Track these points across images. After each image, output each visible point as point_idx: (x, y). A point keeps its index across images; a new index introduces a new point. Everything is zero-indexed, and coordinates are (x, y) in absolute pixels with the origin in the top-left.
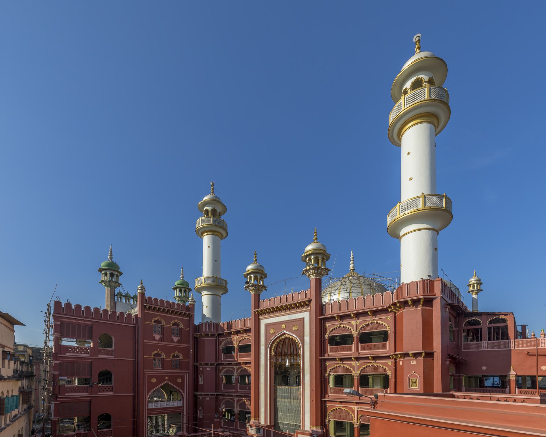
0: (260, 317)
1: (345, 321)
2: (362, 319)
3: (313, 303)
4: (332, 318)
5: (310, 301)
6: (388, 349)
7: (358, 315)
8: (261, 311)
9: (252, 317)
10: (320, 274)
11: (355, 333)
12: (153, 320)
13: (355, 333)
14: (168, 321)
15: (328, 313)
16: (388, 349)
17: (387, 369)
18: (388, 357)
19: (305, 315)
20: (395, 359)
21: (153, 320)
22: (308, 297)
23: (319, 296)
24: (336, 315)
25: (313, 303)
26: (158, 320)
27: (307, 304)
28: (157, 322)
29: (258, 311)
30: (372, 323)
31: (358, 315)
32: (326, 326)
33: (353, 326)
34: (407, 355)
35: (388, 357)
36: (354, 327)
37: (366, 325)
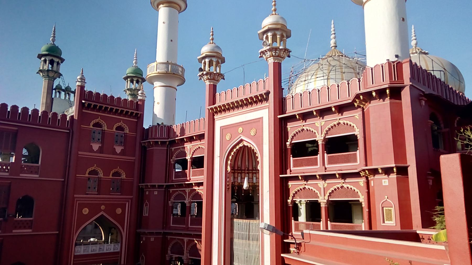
0: (215, 117)
1: (309, 121)
2: (328, 118)
3: (271, 96)
4: (292, 118)
5: (268, 93)
6: (359, 162)
7: (323, 112)
8: (216, 108)
9: (206, 115)
10: (278, 56)
11: (320, 138)
12: (92, 123)
13: (320, 138)
14: (110, 123)
15: (290, 111)
16: (359, 162)
17: (359, 193)
18: (357, 175)
19: (264, 114)
20: (367, 178)
21: (92, 123)
22: (267, 89)
23: (279, 88)
24: (296, 113)
25: (271, 96)
26: (98, 122)
27: (263, 98)
28: (97, 125)
29: (212, 109)
30: (339, 124)
31: (323, 112)
32: (287, 128)
33: (317, 128)
34: (374, 172)
35: (357, 175)
36: (319, 130)
37: (332, 127)
